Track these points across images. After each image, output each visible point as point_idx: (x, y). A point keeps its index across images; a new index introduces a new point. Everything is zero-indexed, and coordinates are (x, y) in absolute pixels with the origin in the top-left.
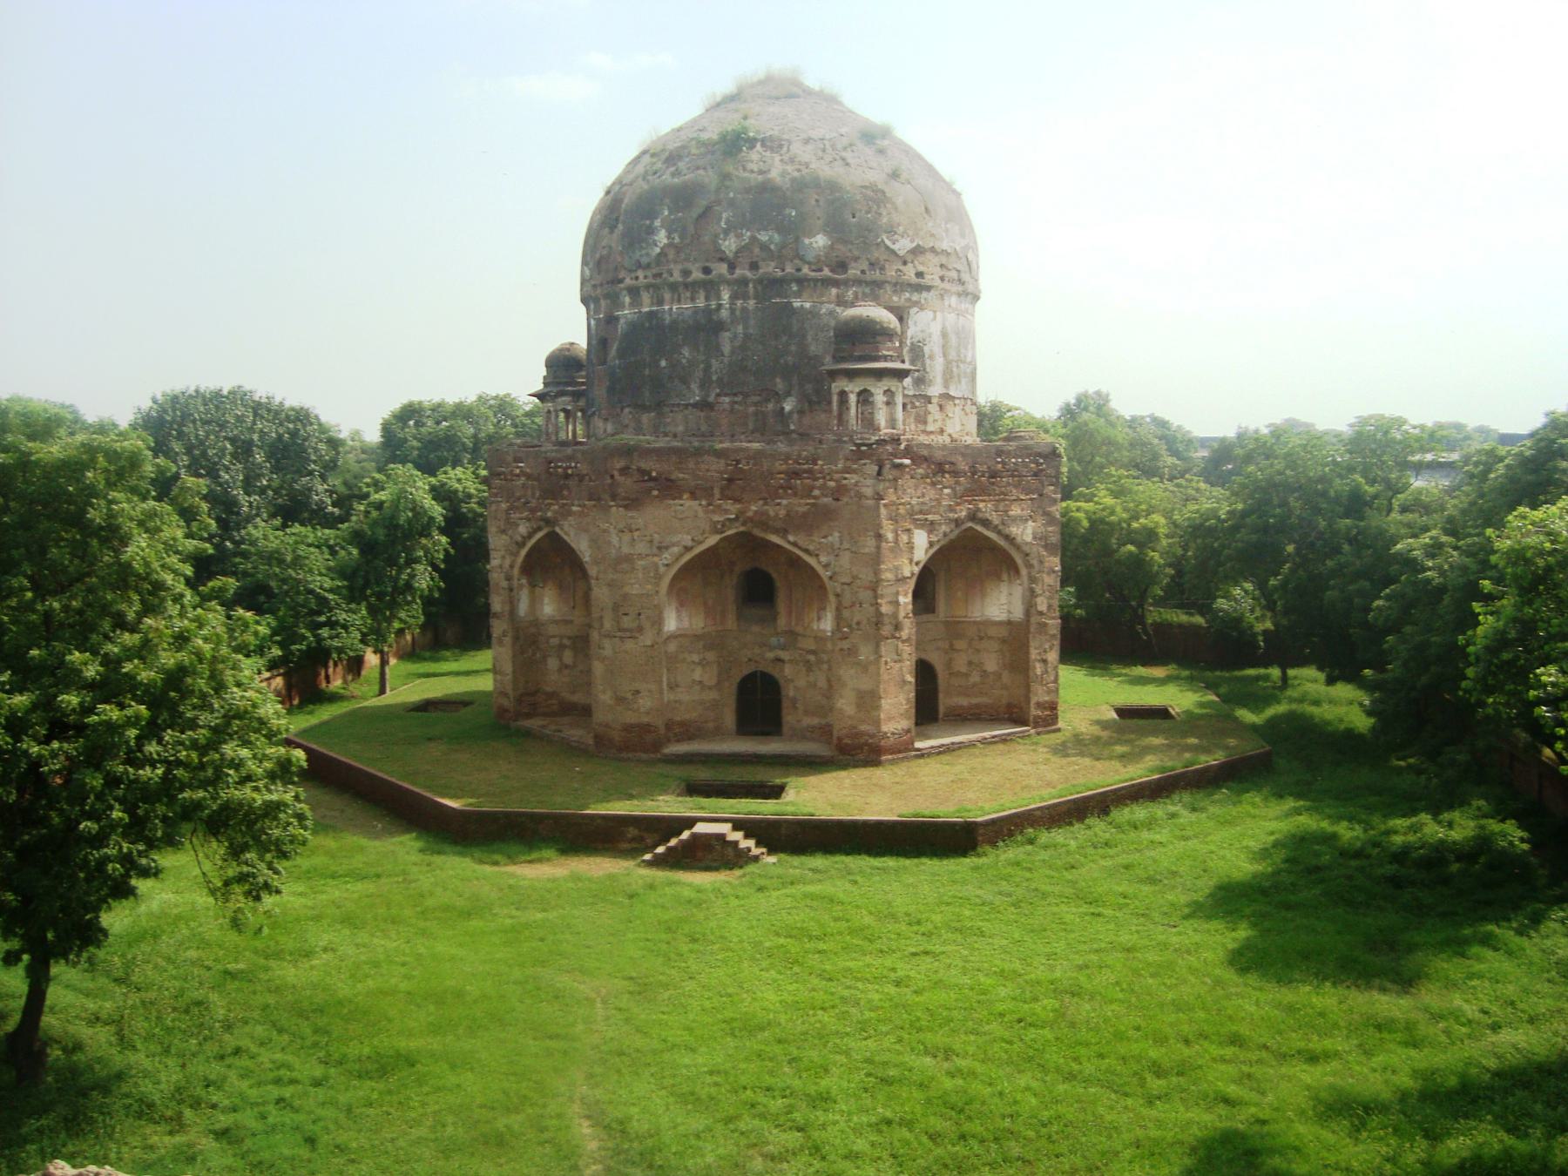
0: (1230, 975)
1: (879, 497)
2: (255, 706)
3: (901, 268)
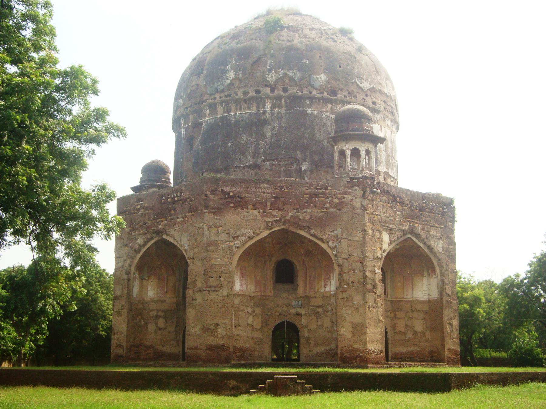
1: (364, 209)
3: (365, 98)
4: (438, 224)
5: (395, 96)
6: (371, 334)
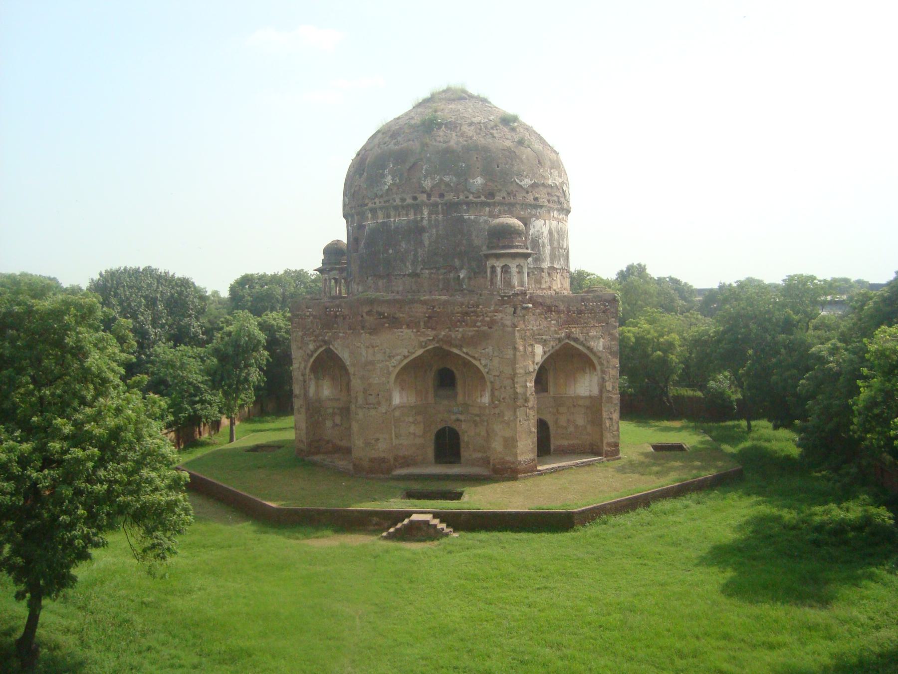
0: (722, 599)
1: (514, 326)
2: (159, 447)
3: (526, 195)
4: (599, 323)
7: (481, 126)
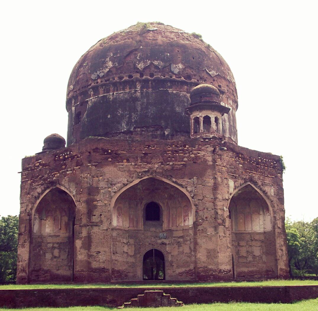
1: (214, 161)
3: (213, 82)
5: (234, 83)
6: (221, 258)
7: (179, 34)
